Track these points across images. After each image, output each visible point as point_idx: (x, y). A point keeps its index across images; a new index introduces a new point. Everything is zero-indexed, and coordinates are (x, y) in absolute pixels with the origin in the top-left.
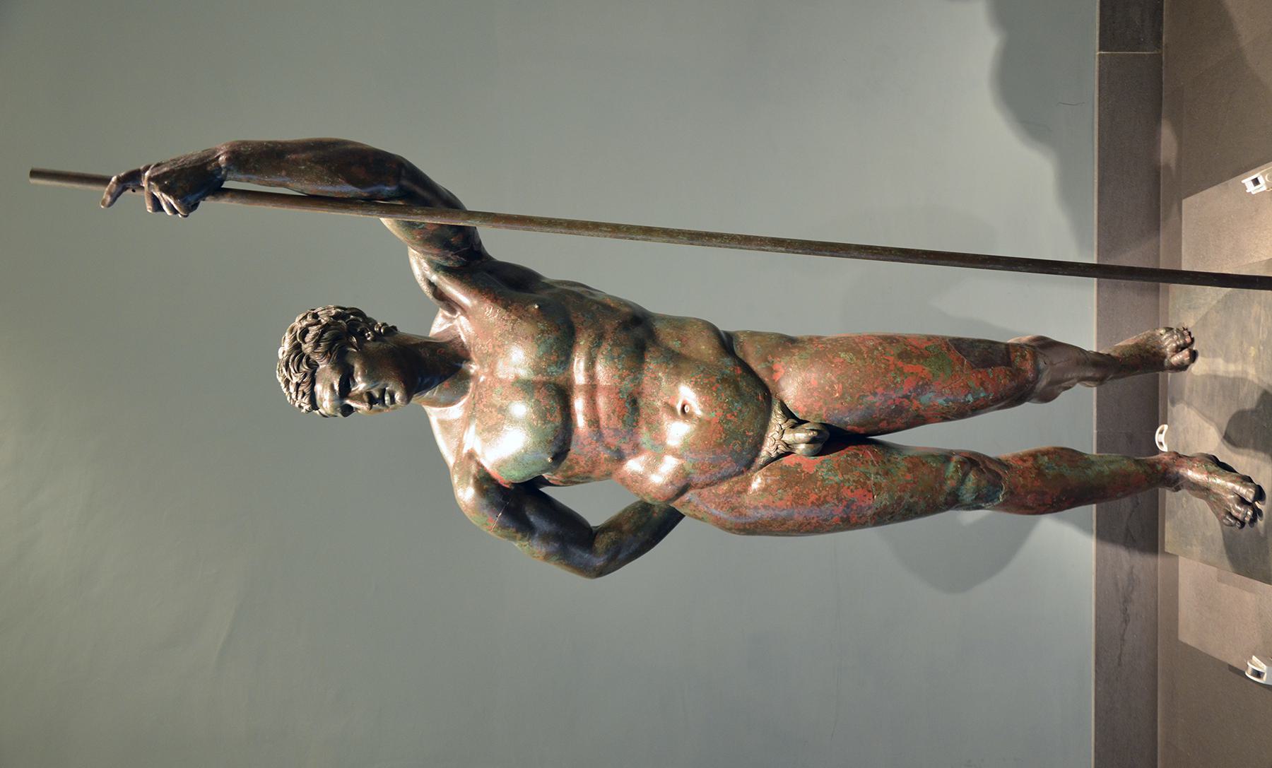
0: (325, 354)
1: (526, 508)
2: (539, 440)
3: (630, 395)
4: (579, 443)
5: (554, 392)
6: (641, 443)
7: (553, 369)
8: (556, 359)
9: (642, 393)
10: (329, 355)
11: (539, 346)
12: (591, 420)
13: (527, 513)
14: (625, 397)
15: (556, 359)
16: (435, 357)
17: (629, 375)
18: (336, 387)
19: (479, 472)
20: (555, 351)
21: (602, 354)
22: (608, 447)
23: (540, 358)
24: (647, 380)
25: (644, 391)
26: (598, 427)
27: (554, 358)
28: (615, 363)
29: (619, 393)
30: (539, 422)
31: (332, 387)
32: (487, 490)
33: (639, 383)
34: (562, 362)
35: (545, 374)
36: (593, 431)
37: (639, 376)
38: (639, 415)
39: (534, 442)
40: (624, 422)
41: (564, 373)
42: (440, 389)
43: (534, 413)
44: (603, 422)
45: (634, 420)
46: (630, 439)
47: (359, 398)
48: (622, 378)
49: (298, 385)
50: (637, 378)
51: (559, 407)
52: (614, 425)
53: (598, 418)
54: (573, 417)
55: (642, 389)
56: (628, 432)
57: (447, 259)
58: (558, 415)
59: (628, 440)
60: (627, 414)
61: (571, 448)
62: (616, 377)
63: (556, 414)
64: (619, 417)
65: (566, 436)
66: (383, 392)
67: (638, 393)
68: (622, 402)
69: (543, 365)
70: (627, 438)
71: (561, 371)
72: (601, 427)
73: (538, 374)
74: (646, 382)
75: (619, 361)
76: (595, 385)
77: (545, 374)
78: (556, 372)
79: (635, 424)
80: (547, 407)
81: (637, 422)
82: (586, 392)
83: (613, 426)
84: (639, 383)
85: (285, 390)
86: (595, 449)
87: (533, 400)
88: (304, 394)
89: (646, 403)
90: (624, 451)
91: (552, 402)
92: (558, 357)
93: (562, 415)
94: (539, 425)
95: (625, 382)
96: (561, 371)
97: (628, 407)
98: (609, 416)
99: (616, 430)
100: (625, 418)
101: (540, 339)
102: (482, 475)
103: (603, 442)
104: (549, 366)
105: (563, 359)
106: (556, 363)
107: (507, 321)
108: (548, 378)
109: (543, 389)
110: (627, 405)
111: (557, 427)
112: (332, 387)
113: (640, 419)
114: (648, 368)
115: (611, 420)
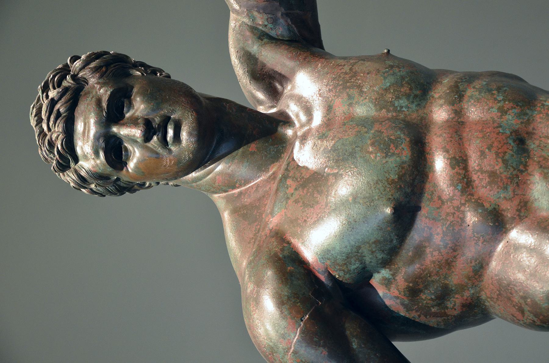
0: (96, 70)
1: (347, 325)
2: (375, 178)
3: (515, 132)
4: (436, 198)
5: (402, 126)
6: (532, 198)
7: (403, 102)
8: (408, 92)
9: (534, 134)
10: (104, 69)
11: (385, 78)
12: (454, 158)
13: (348, 332)
14: (508, 132)
15: (408, 92)
16: (243, 114)
17: (512, 108)
18: (104, 105)
19: (282, 250)
20: (408, 83)
21: (474, 87)
22: (478, 204)
23: (386, 89)
24: (541, 118)
25: (536, 132)
26: (466, 168)
27: (405, 89)
28: (493, 94)
29: (497, 127)
30: (378, 154)
31: (99, 102)
32: (291, 274)
33: (528, 120)
34: (416, 96)
35: (391, 108)
36: (457, 173)
37: (528, 111)
38: (529, 157)
39: (368, 183)
40: (505, 162)
41: (417, 111)
42: (243, 152)
43: (373, 144)
44: (474, 162)
45: (521, 163)
46: (514, 191)
47: (134, 122)
48: (503, 111)
49: (53, 103)
50: (525, 114)
51: (408, 140)
52: (489, 165)
53: (466, 156)
54: (428, 156)
55: (534, 129)
56: (511, 178)
57: (274, 21)
58: (405, 148)
59: (510, 194)
60: (511, 153)
61: (423, 205)
62: (495, 110)
63: (402, 146)
64: (497, 154)
65: (416, 182)
66: (166, 120)
67: (527, 133)
68: (504, 138)
69: (389, 97)
70: (510, 188)
71: (414, 106)
72: (470, 169)
73: (381, 109)
74: (539, 120)
75: (499, 92)
76: (463, 122)
77: (391, 108)
78: (407, 107)
79: (521, 167)
80: (392, 137)
81: (526, 166)
82: (449, 127)
83: (488, 168)
84: (528, 120)
85: (32, 106)
86: (458, 208)
87: (372, 132)
88: (59, 115)
89: (538, 146)
90: (505, 214)
91: (399, 133)
92: (411, 89)
93: (412, 149)
94: (378, 158)
95: (507, 117)
96: (414, 106)
97: (512, 144)
98: (482, 154)
99: (493, 175)
100: (507, 157)
101: (387, 72)
102: (286, 253)
103: (472, 195)
104: (398, 98)
105: (418, 92)
106: (408, 96)
107: (344, 65)
108: (394, 114)
109: (387, 122)
110: (511, 142)
111: (403, 163)
112: (99, 102)
113: (530, 162)
114: (543, 105)
115: (485, 158)
